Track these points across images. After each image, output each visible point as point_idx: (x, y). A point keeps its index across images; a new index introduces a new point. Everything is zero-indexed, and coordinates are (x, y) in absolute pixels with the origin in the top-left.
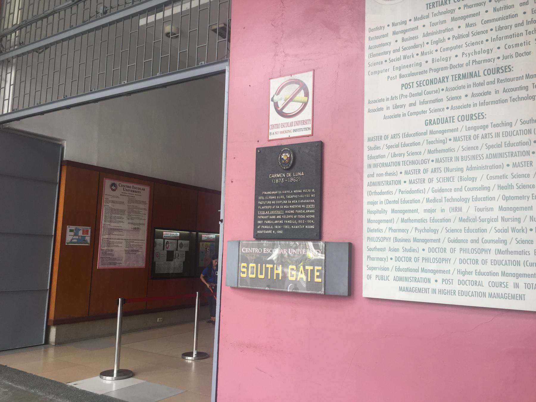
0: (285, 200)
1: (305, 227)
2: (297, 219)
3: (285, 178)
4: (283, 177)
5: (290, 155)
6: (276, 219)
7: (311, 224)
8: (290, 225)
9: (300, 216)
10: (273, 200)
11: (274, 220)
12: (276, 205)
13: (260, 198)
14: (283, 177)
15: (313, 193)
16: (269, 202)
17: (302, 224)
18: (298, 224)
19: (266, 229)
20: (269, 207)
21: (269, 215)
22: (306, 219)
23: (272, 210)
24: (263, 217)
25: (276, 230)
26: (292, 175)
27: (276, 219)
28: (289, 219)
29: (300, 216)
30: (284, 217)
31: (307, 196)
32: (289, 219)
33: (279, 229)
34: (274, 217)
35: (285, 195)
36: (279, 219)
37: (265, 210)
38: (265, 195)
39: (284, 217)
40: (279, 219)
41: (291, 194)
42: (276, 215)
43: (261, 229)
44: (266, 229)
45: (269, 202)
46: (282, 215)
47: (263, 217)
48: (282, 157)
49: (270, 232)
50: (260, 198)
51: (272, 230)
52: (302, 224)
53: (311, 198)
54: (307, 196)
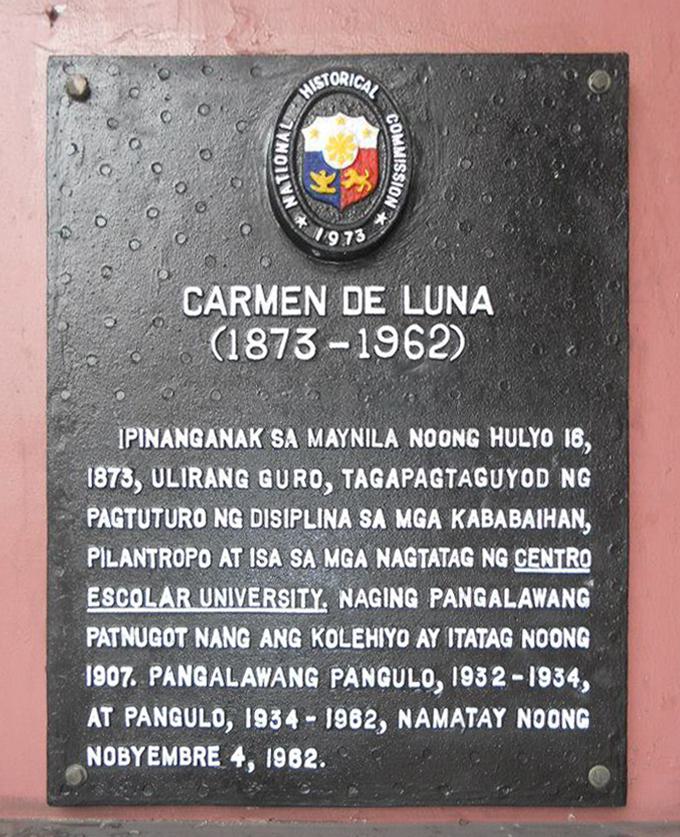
0: (334, 502)
1: (510, 718)
2: (444, 659)
3: (330, 325)
4: (301, 320)
5: (384, 136)
6: (256, 656)
7: (564, 698)
8: (387, 702)
9: (470, 637)
10: (225, 496)
11: (235, 660)
12: (245, 538)
13: (99, 476)
14: (301, 320)
15: (573, 459)
16: (183, 516)
17: (485, 697)
18: (456, 697)
19: (167, 737)
20: (188, 553)
21: (191, 620)
22: (515, 659)
23: (218, 576)
24: (130, 636)
25: (258, 742)
26: (389, 299)
27: (256, 656)
28: (372, 657)
29: (470, 637)
30: (333, 638)
31: (533, 478)
32: (372, 657)
33: (286, 738)
34: (236, 638)
35: (329, 460)
36: (283, 657)
37: (154, 578)
38: (141, 459)
39: (333, 638)
40: (283, 657)
41: (386, 459)
42: (256, 624)
43: (116, 734)
44: (167, 737)
45: (183, 516)
46: (305, 624)
47: (130, 636)
48: (311, 144)
49: (207, 755)
50: (99, 476)
51: (226, 742)
52: (485, 697)
53: (556, 497)
54: (533, 478)
